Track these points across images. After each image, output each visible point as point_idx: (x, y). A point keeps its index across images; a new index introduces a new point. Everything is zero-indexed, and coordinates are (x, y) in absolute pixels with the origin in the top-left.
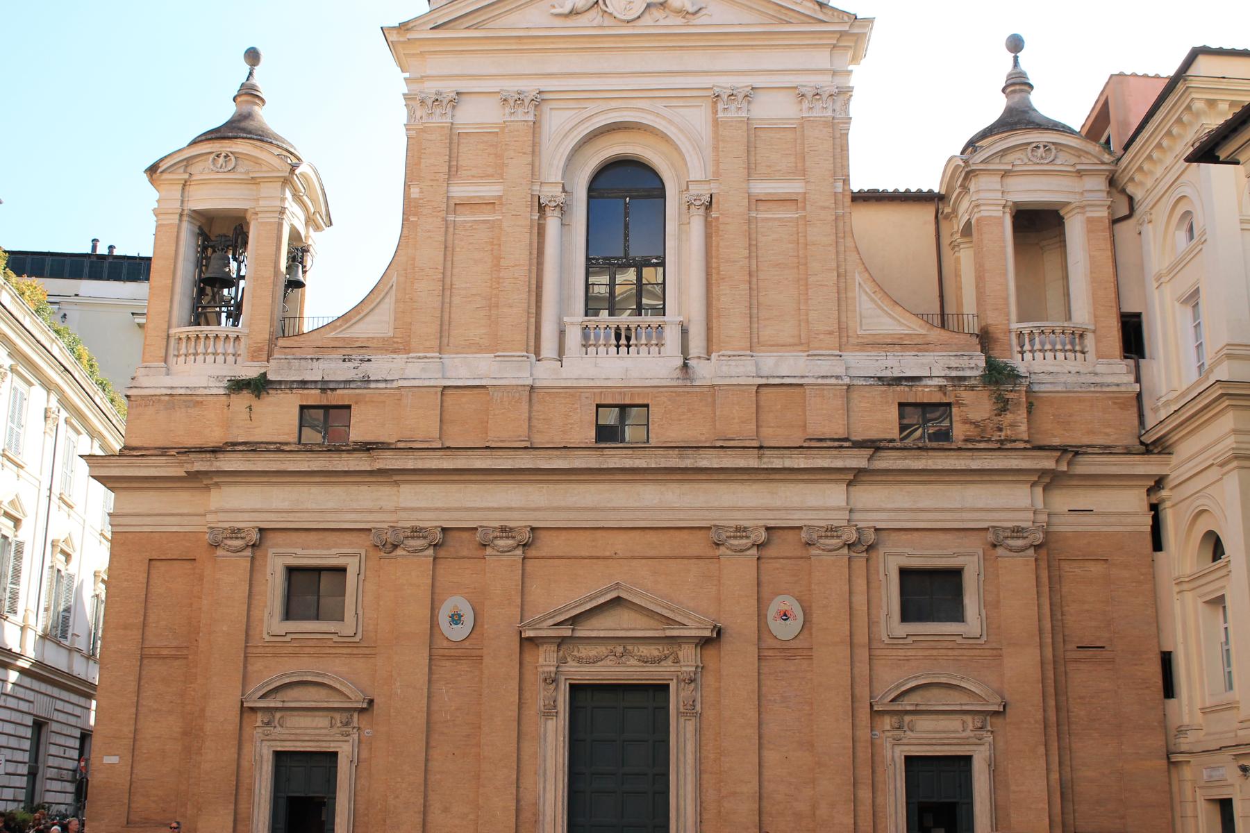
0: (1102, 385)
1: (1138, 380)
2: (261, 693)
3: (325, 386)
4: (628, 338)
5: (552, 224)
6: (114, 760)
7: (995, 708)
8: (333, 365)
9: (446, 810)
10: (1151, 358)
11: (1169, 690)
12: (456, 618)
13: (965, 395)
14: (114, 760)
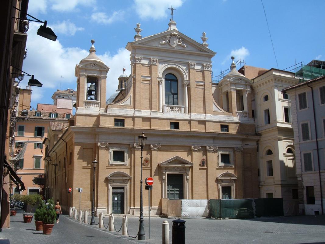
5: (161, 85)
11: (259, 175)
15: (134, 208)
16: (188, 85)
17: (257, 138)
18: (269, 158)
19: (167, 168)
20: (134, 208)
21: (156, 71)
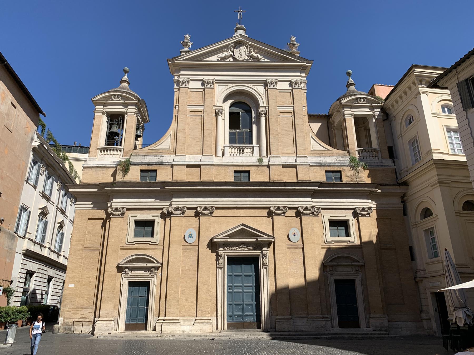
0: (385, 166)
1: (395, 165)
2: (125, 262)
3: (149, 164)
4: (243, 151)
6: (73, 285)
7: (362, 264)
8: (151, 158)
9: (186, 300)
10: (397, 159)
11: (413, 258)
12: (190, 236)
13: (345, 168)
14: (73, 285)
15: (164, 320)
16: (265, 114)
17: (401, 190)
18: (428, 223)
19: (225, 245)
20: (164, 320)
21: (212, 97)
